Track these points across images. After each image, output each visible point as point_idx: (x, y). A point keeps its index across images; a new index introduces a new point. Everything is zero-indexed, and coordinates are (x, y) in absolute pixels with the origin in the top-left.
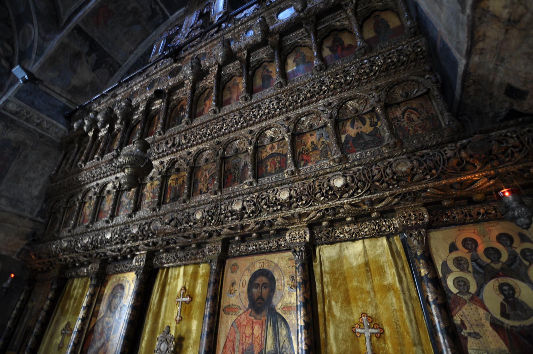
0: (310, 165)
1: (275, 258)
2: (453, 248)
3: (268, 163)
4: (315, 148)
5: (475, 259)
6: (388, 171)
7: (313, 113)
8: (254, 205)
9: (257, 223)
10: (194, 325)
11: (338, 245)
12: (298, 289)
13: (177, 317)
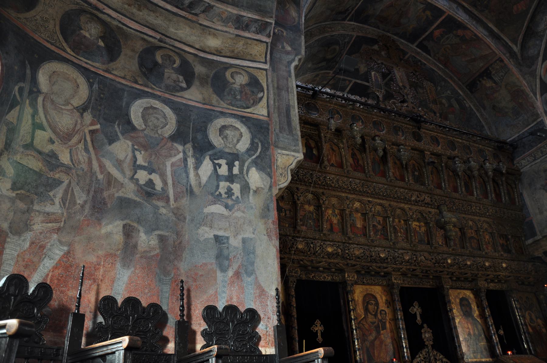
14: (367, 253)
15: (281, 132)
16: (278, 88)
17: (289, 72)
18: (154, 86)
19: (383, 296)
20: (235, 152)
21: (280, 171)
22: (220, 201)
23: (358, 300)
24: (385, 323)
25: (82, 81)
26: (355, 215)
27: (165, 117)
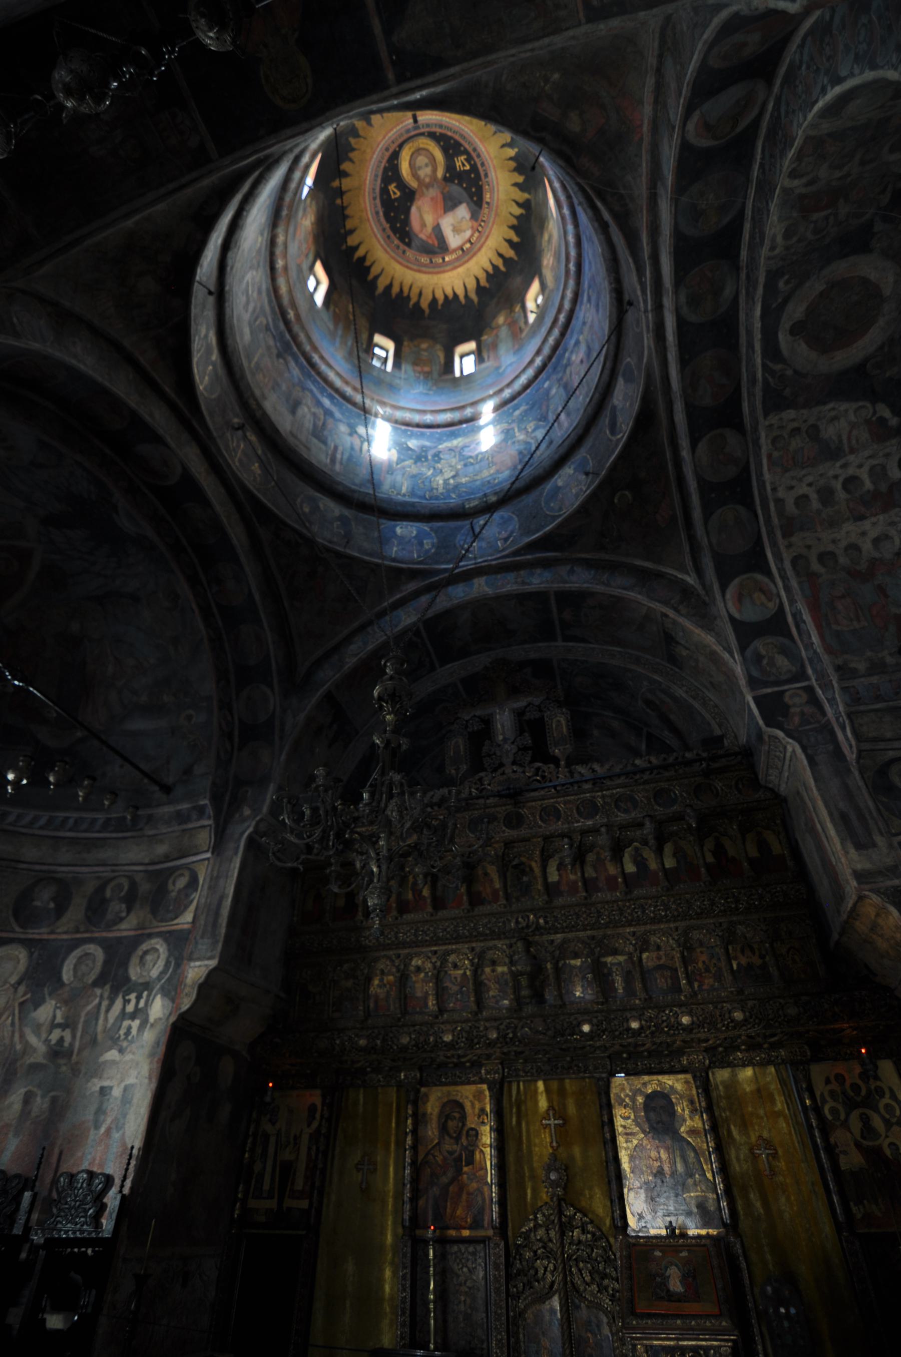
0: (705, 987)
1: (668, 1081)
2: (828, 1081)
3: (657, 976)
4: (707, 970)
5: (844, 1093)
6: (780, 1012)
7: (703, 929)
8: (654, 1026)
9: (654, 1043)
10: (577, 1151)
11: (729, 1070)
12: (704, 1115)
13: (551, 1142)
14: (422, 1039)
15: (202, 937)
16: (218, 877)
17: (238, 847)
18: (94, 929)
19: (476, 1102)
20: (147, 979)
21: (186, 991)
22: (116, 1044)
23: (431, 1114)
24: (472, 1153)
25: (22, 955)
26: (414, 979)
27: (94, 961)
